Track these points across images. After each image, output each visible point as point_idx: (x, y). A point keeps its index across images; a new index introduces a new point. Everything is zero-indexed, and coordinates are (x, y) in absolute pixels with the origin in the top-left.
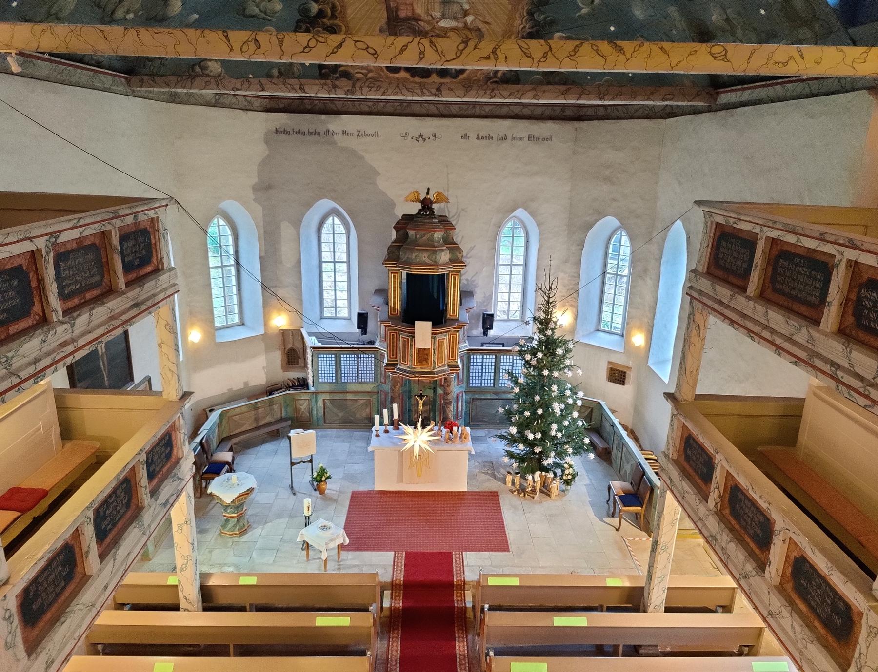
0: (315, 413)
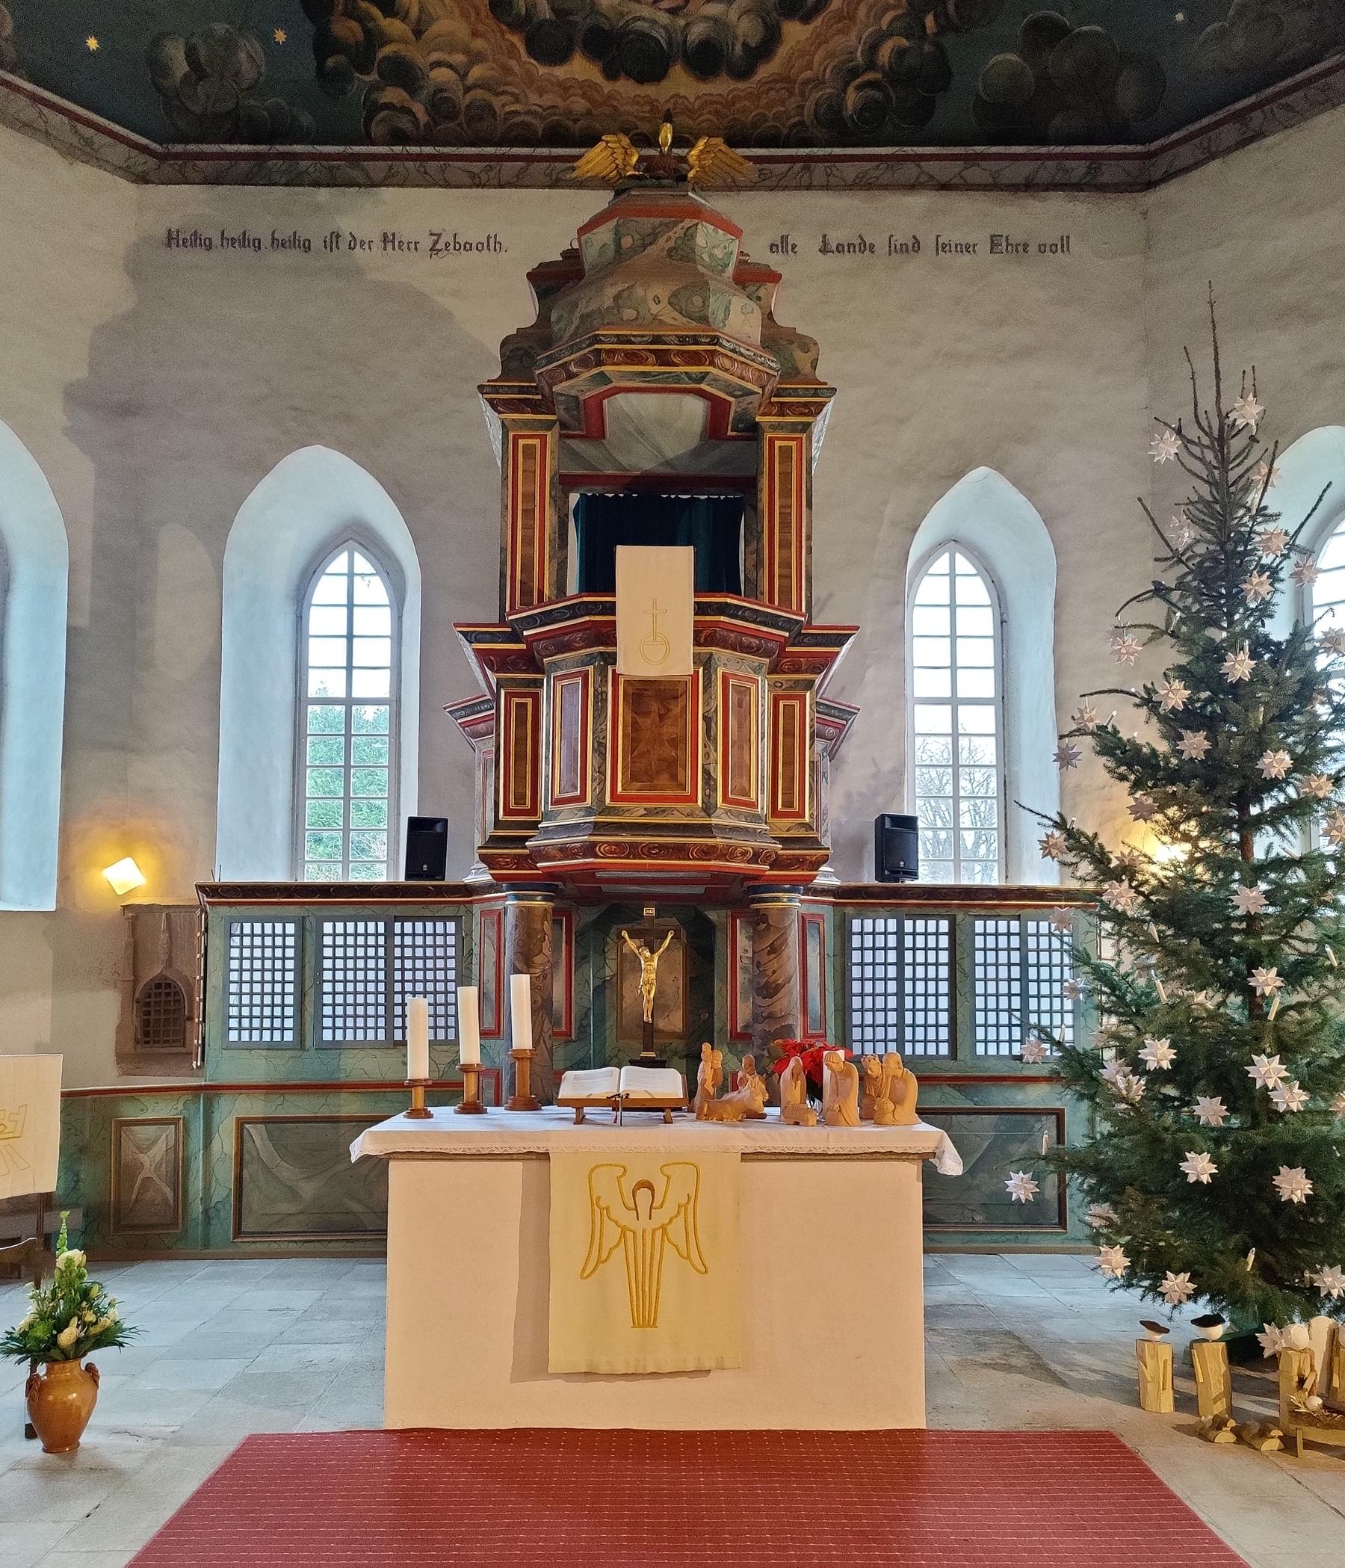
0: (197, 1185)
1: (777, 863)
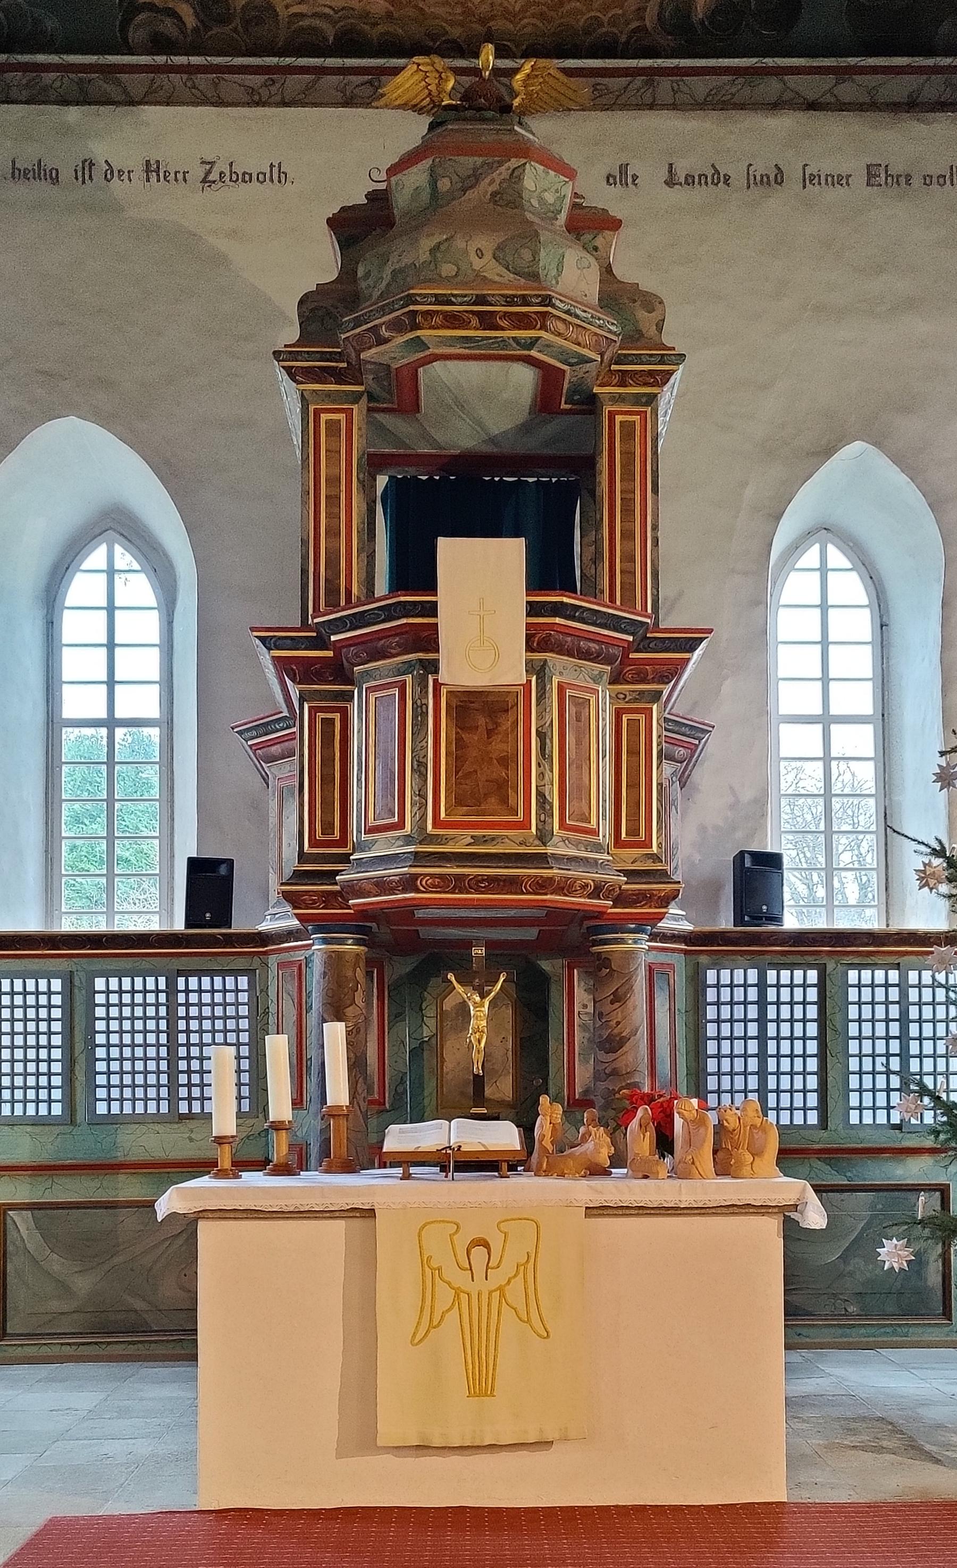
1: (621, 899)
